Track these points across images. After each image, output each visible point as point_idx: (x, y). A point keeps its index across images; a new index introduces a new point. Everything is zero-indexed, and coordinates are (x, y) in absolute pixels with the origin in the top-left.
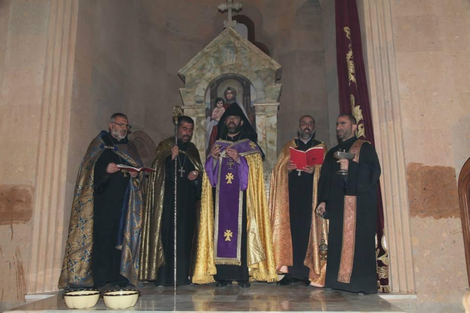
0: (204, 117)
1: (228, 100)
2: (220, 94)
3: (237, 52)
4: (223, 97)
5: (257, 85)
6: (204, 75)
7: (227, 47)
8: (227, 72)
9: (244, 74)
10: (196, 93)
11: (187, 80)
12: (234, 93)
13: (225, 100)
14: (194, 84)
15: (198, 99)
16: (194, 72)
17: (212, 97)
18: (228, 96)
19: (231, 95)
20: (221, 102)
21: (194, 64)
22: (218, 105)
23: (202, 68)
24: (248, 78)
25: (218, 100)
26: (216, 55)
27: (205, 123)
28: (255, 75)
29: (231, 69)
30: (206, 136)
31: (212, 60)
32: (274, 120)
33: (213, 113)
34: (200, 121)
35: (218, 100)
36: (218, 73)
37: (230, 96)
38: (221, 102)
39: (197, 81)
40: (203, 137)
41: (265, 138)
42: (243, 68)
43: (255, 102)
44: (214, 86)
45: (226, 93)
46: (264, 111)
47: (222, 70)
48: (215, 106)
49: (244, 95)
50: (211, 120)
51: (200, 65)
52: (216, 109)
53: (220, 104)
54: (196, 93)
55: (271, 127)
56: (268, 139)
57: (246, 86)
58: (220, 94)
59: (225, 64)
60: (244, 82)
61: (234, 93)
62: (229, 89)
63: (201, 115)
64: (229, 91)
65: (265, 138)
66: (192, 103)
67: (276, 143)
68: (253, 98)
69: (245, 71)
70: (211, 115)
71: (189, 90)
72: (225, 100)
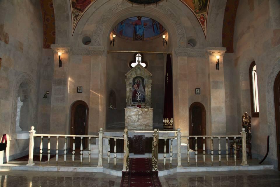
5: (146, 80)
6: (132, 76)
7: (138, 69)
8: (138, 76)
9: (142, 76)
10: (130, 81)
11: (127, 77)
12: (140, 81)
14: (129, 78)
15: (130, 83)
16: (129, 75)
17: (134, 82)
23: (131, 74)
24: (144, 77)
26: (135, 71)
28: (145, 77)
30: (132, 92)
31: (134, 72)
32: (150, 89)
35: (135, 83)
36: (136, 76)
37: (139, 82)
39: (130, 78)
40: (131, 93)
41: (148, 94)
42: (142, 75)
43: (145, 84)
44: (134, 79)
45: (137, 81)
46: (148, 87)
47: (137, 75)
48: (134, 85)
51: (131, 73)
52: (135, 86)
53: (136, 84)
54: (130, 81)
55: (149, 91)
57: (143, 79)
58: (136, 81)
61: (140, 81)
62: (138, 80)
63: (131, 87)
65: (148, 94)
66: (128, 84)
67: (150, 96)
68: (145, 83)
69: (143, 76)
71: (128, 80)
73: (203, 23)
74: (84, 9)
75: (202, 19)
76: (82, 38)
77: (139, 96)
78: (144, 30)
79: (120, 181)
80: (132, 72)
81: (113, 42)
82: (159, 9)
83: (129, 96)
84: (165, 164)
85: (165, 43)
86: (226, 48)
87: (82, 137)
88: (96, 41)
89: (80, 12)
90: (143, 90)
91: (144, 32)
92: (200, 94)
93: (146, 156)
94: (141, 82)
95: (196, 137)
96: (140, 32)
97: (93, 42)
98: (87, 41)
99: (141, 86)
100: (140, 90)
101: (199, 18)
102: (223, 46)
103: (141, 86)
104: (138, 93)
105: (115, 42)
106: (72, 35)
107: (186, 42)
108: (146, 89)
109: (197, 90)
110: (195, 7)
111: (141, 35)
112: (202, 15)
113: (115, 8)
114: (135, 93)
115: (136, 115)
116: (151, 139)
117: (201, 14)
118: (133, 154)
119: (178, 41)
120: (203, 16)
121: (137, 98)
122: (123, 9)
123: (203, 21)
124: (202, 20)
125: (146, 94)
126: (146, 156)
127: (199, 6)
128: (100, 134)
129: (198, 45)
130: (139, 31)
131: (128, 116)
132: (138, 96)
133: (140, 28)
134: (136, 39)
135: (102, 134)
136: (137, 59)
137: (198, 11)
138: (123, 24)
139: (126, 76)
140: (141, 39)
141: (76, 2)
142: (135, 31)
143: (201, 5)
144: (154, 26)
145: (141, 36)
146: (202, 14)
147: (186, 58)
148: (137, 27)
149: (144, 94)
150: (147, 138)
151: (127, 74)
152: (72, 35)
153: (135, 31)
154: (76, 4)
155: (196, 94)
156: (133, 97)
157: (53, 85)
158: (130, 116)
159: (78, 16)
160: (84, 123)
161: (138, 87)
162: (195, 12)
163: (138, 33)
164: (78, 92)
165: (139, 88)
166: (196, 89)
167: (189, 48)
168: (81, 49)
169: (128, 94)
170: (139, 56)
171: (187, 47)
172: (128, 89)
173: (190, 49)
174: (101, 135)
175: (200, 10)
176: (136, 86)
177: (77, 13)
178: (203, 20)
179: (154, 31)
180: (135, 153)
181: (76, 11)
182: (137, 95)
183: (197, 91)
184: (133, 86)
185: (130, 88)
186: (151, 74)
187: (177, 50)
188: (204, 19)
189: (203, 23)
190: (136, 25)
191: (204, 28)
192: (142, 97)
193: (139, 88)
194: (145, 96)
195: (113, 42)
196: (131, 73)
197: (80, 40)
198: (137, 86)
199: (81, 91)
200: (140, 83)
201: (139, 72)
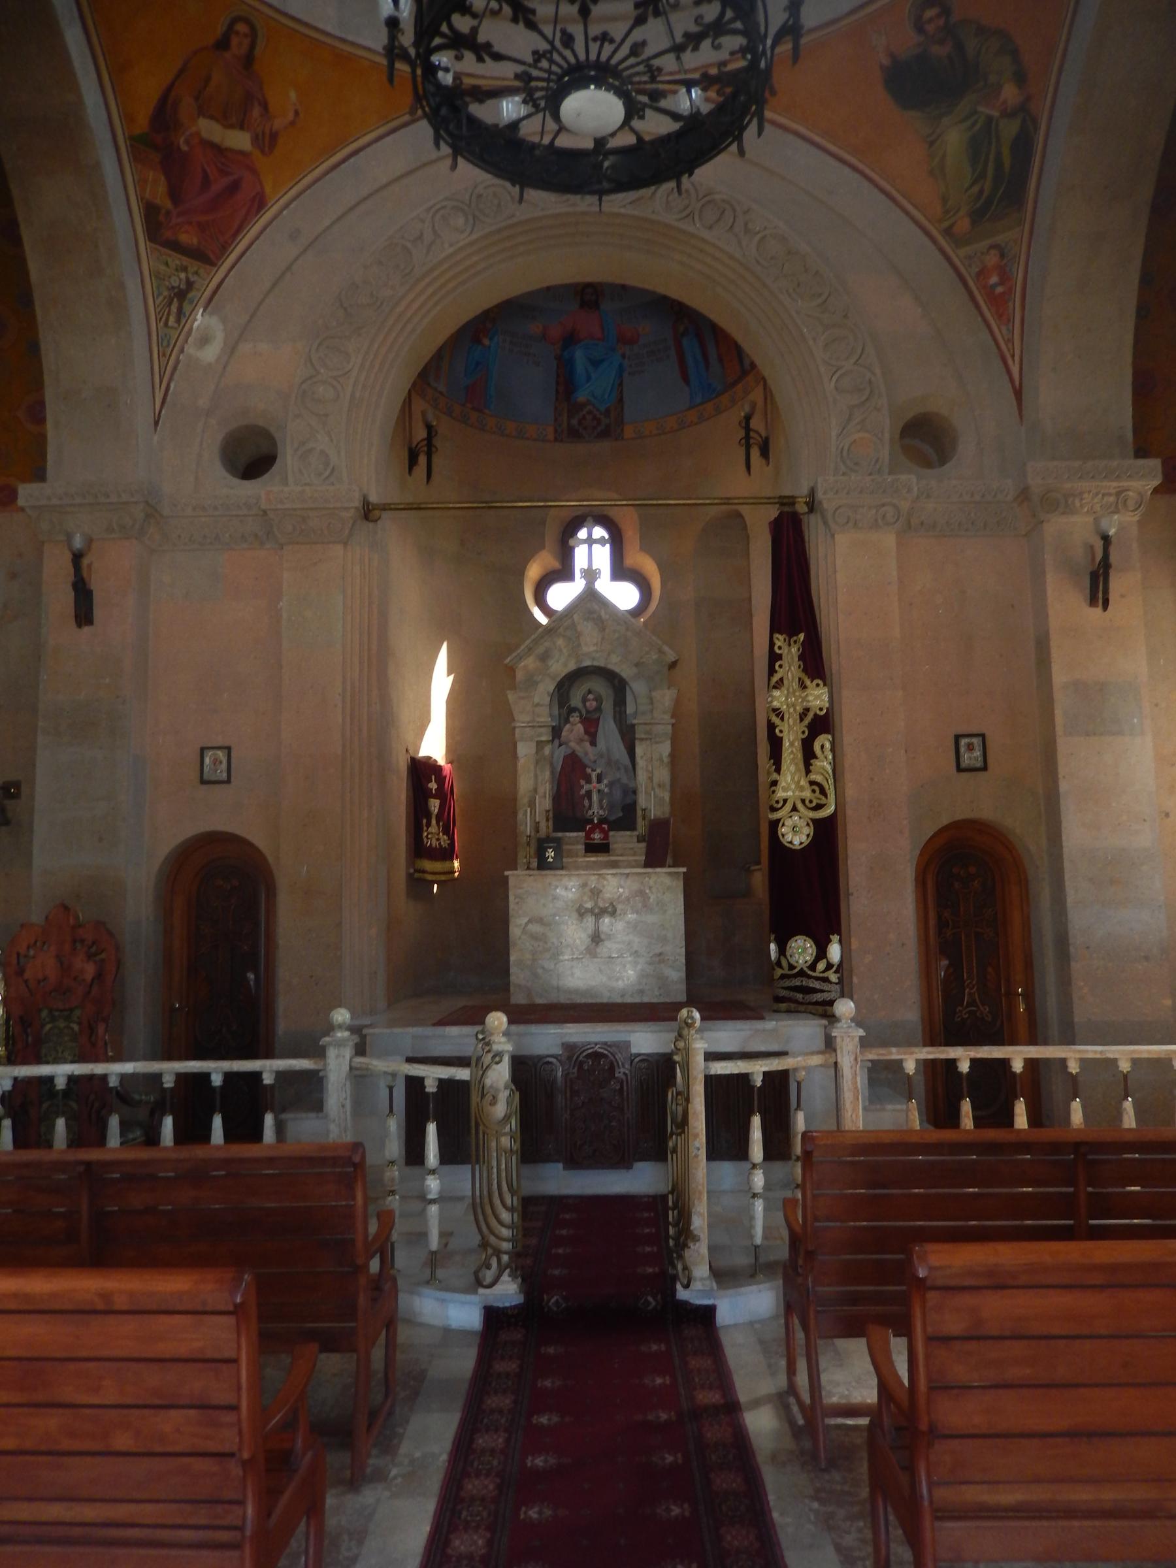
0: (548, 742)
1: (588, 712)
2: (576, 701)
3: (604, 629)
4: (580, 705)
5: (638, 687)
8: (587, 663)
11: (520, 675)
12: (599, 699)
13: (584, 712)
14: (531, 683)
17: (561, 706)
18: (588, 704)
19: (594, 703)
20: (577, 714)
21: (530, 649)
22: (571, 719)
25: (572, 710)
27: (552, 753)
29: (594, 659)
30: (552, 773)
32: (665, 749)
33: (563, 734)
34: (543, 748)
35: (572, 710)
36: (572, 666)
37: (591, 705)
38: (577, 714)
40: (547, 774)
41: (651, 779)
45: (584, 700)
48: (567, 721)
49: (615, 704)
50: (560, 745)
51: (540, 650)
52: (568, 726)
53: (575, 718)
55: (661, 760)
56: (656, 780)
58: (576, 701)
59: (585, 649)
60: (616, 681)
61: (599, 699)
62: (590, 692)
63: (544, 738)
64: (591, 696)
65: (651, 779)
67: (668, 787)
68: (630, 709)
70: (559, 737)
72: (584, 712)
73: (999, 303)
74: (224, 249)
75: (994, 279)
76: (220, 437)
77: (599, 791)
78: (621, 369)
79: (464, 1362)
80: (547, 644)
81: (422, 460)
82: (711, 228)
83: (535, 790)
84: (758, 1240)
85: (755, 453)
86: (1155, 464)
87: (216, 1070)
88: (310, 451)
89: (201, 271)
90: (619, 751)
91: (621, 384)
92: (985, 768)
93: (639, 1180)
94: (608, 706)
95: (963, 1057)
96: (594, 388)
97: (288, 458)
98: (252, 457)
99: (608, 728)
100: (601, 756)
101: (975, 270)
102: (1141, 452)
103: (608, 728)
104: (594, 775)
105: (436, 459)
106: (156, 423)
107: (887, 436)
108: (639, 750)
109: (963, 742)
110: (944, 200)
111: (602, 409)
112: (993, 252)
113: (420, 237)
114: (571, 774)
115: (581, 913)
116: (662, 1071)
117: (984, 244)
118: (560, 1166)
119: (834, 433)
120: (1002, 256)
121: (586, 802)
122: (474, 237)
123: (1000, 289)
124: (996, 285)
125: (642, 776)
126: (639, 1180)
127: (976, 189)
128: (331, 1053)
129: (966, 448)
130: (589, 379)
131: (530, 921)
132: (589, 794)
133: (596, 363)
134: (574, 434)
135: (348, 1052)
136: (580, 556)
137: (963, 225)
138: (486, 342)
139: (511, 670)
140: (605, 434)
141: (169, 204)
142: (566, 384)
143: (988, 185)
144: (685, 342)
145: (608, 411)
146: (992, 247)
147: (889, 540)
148: (579, 356)
149: (625, 780)
150: (646, 1058)
151: (520, 658)
152: (156, 423)
153: (566, 384)
154: (168, 213)
155: (960, 769)
156: (557, 799)
157: (41, 740)
158: (540, 921)
159: (190, 295)
160: (251, 976)
161: (592, 734)
162: (948, 232)
163: (581, 396)
164: (203, 782)
165: (593, 743)
166: (957, 738)
167: (903, 477)
168: (216, 508)
169: (525, 784)
170: (590, 541)
171: (890, 473)
172: (525, 750)
173: (913, 478)
174: (337, 1056)
175: (979, 215)
176: (575, 730)
177: (183, 275)
178: (1001, 283)
179: (685, 378)
180: (574, 1162)
181: (176, 260)
182: (587, 787)
183: (962, 750)
184: (556, 732)
185: (540, 745)
186: (666, 648)
187: (825, 493)
188: (1005, 277)
189: (999, 303)
190: (570, 339)
191: (1009, 341)
192: (618, 794)
193: (593, 743)
194: (635, 792)
195: (422, 460)
196: (540, 650)
197: (207, 444)
198: (586, 732)
199: (224, 776)
200: (598, 709)
201: (593, 649)
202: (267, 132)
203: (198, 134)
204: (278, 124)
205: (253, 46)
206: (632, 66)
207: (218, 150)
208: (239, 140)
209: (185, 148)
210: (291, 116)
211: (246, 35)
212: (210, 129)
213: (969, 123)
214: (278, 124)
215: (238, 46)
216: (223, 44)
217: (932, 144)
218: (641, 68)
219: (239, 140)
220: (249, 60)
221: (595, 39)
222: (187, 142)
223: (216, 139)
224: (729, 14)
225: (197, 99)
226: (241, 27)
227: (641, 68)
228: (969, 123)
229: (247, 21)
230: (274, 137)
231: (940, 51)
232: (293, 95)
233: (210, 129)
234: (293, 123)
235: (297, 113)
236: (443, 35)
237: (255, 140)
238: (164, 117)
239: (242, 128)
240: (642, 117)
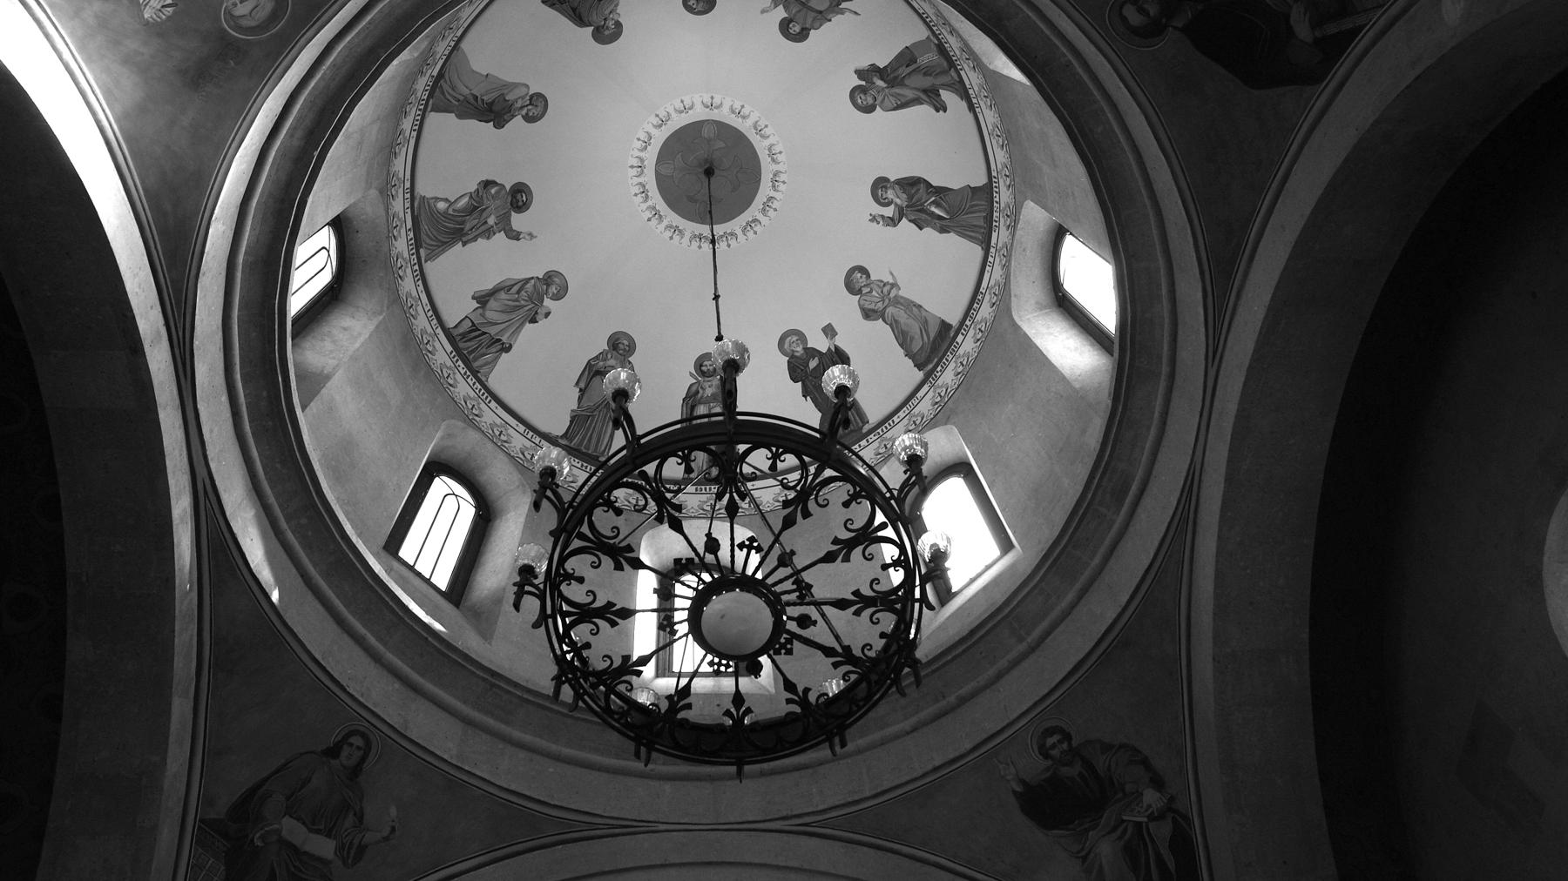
202: (356, 842)
203: (278, 832)
204: (369, 837)
205: (363, 759)
206: (781, 581)
207: (294, 850)
208: (324, 847)
209: (258, 843)
210: (386, 832)
211: (359, 748)
212: (292, 830)
213: (1119, 832)
214: (369, 837)
215: (348, 757)
216: (333, 752)
217: (1084, 859)
218: (788, 585)
219: (324, 847)
220: (356, 771)
221: (741, 546)
222: (262, 838)
223: (297, 842)
224: (880, 518)
225: (288, 799)
226: (357, 741)
227: (788, 585)
228: (1119, 832)
229: (363, 735)
230: (362, 849)
231: (1072, 771)
232: (393, 811)
233: (292, 830)
234: (386, 839)
235: (393, 829)
236: (582, 537)
237: (340, 849)
238: (248, 807)
239: (329, 836)
240: (789, 652)
